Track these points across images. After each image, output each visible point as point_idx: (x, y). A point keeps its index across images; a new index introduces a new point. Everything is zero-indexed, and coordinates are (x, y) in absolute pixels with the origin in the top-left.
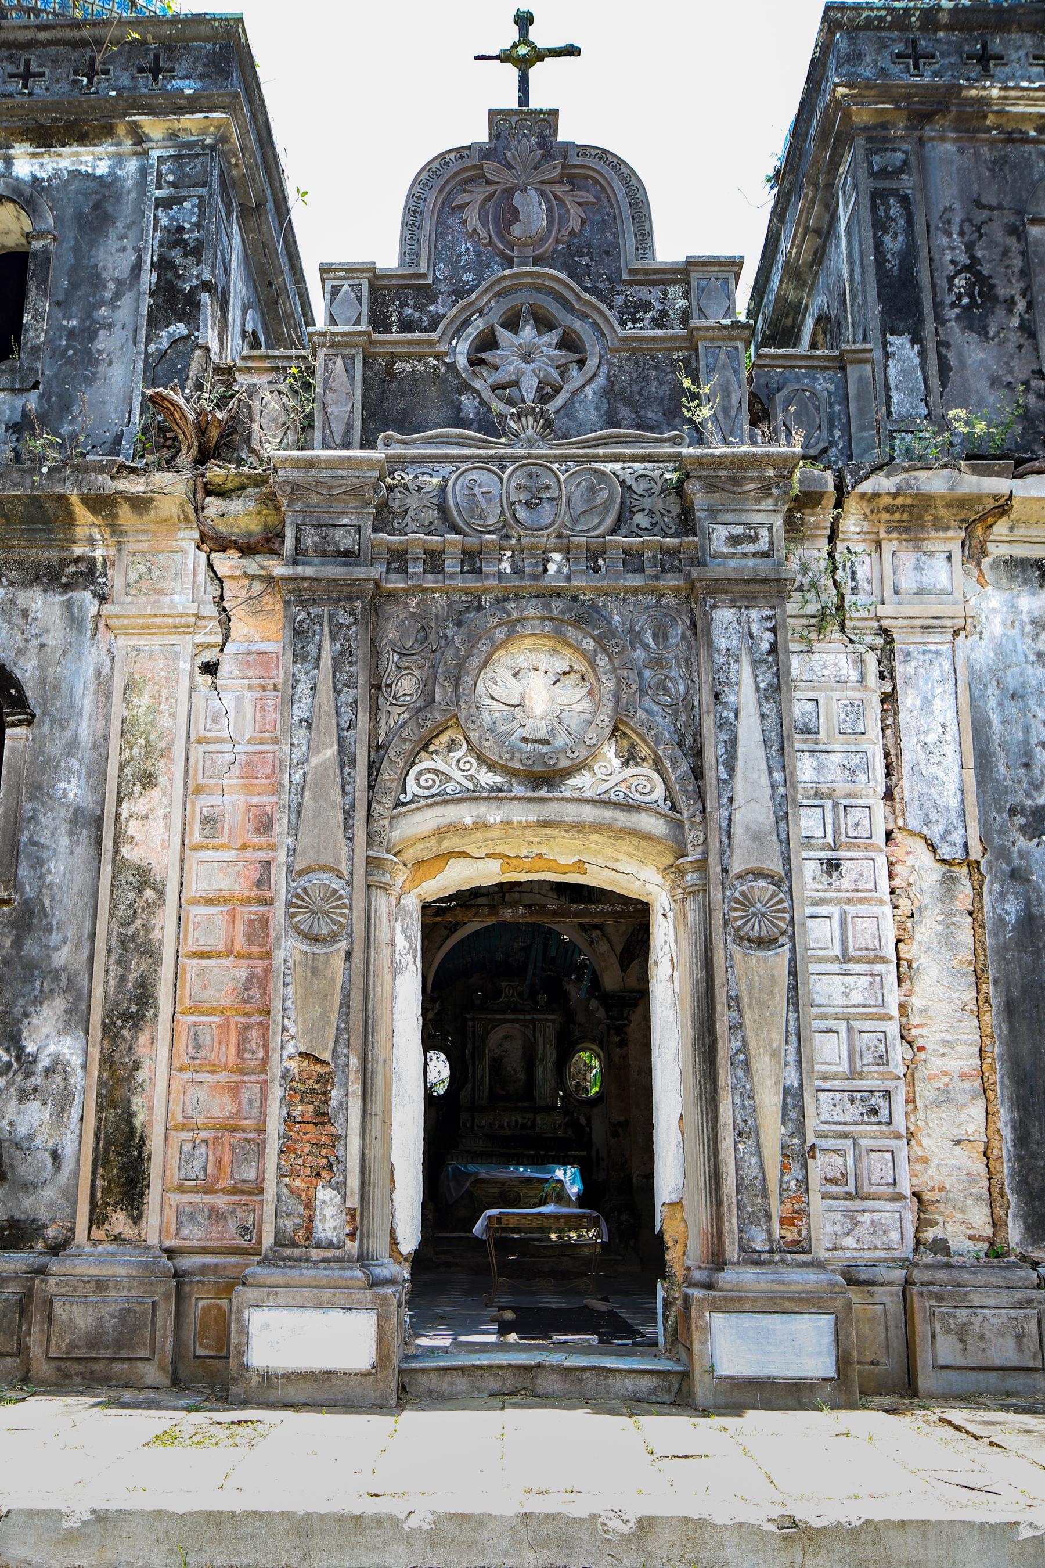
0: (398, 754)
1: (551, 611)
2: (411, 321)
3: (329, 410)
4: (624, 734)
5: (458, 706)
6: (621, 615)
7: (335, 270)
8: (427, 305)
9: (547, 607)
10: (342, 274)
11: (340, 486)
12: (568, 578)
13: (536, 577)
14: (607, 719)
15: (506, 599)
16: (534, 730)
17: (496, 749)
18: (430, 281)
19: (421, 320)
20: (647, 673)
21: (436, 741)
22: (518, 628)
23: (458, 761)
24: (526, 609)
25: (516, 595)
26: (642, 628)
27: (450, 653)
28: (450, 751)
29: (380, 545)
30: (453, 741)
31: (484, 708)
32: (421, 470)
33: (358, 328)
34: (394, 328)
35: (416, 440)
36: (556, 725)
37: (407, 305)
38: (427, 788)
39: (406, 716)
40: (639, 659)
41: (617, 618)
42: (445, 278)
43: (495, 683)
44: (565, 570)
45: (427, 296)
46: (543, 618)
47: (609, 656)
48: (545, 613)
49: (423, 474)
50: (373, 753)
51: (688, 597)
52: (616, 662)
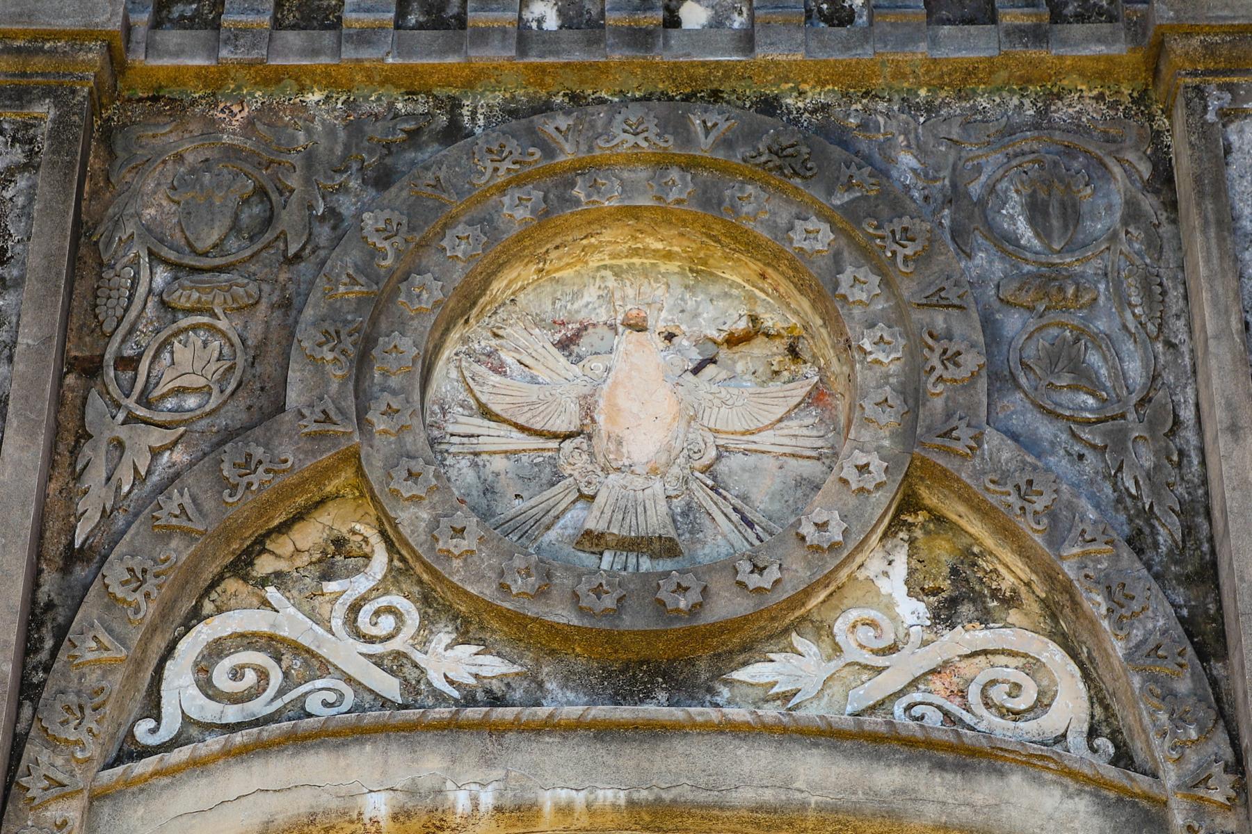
0: (137, 579)
1: (687, 139)
4: (939, 519)
5: (362, 422)
6: (920, 150)
9: (679, 128)
12: (747, 40)
13: (640, 38)
14: (877, 465)
15: (546, 108)
16: (624, 509)
17: (487, 561)
20: (1013, 323)
21: (283, 545)
22: (579, 192)
23: (355, 608)
24: (607, 133)
25: (574, 98)
26: (992, 189)
27: (348, 259)
28: (327, 576)
30: (339, 543)
31: (455, 445)
36: (702, 496)
38: (235, 699)
39: (180, 456)
40: (981, 282)
41: (907, 160)
43: (499, 369)
44: (738, 22)
46: (662, 163)
47: (879, 270)
48: (670, 144)
50: (50, 581)
51: (1141, 99)
52: (908, 289)
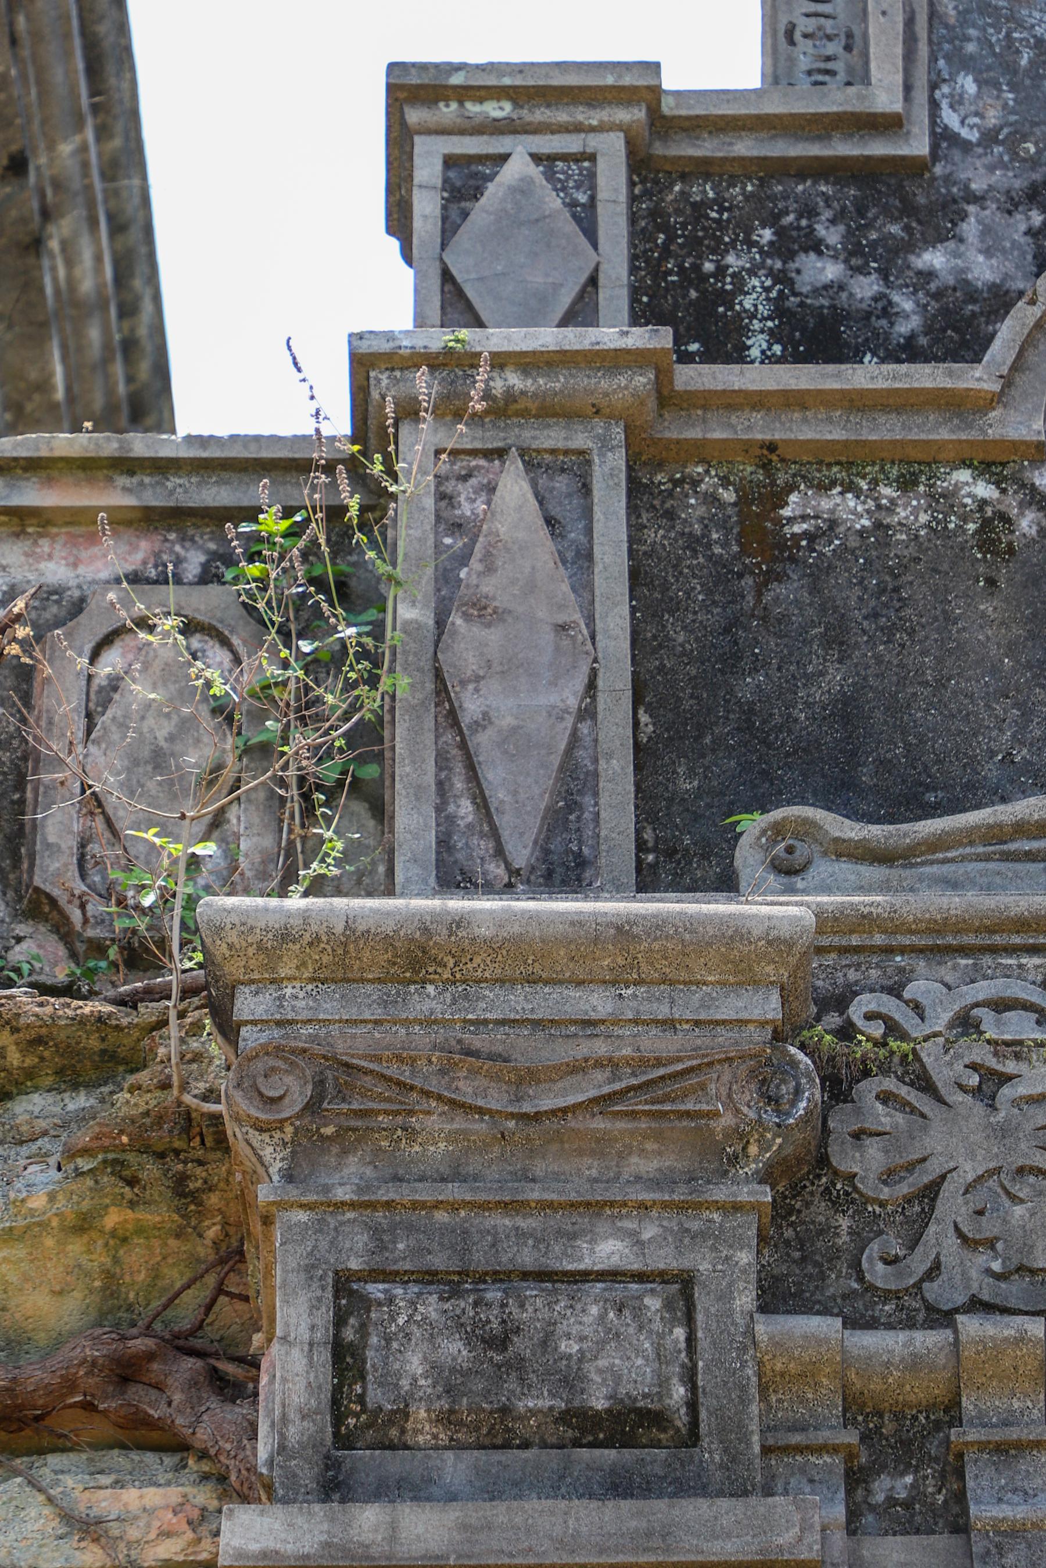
2: (838, 316)
3: (471, 706)
7: (465, 93)
8: (910, 246)
10: (497, 110)
11: (576, 1068)
18: (919, 146)
19: (887, 310)
29: (807, 1375)
32: (983, 990)
33: (576, 339)
34: (757, 345)
35: (936, 844)
37: (816, 247)
42: (989, 138)
45: (908, 209)
49: (1001, 1006)
